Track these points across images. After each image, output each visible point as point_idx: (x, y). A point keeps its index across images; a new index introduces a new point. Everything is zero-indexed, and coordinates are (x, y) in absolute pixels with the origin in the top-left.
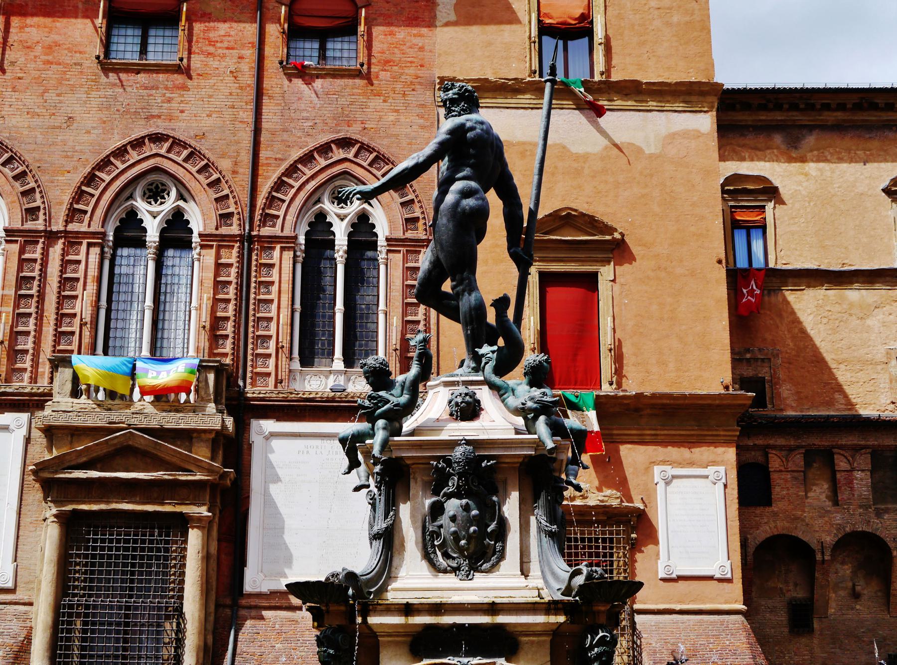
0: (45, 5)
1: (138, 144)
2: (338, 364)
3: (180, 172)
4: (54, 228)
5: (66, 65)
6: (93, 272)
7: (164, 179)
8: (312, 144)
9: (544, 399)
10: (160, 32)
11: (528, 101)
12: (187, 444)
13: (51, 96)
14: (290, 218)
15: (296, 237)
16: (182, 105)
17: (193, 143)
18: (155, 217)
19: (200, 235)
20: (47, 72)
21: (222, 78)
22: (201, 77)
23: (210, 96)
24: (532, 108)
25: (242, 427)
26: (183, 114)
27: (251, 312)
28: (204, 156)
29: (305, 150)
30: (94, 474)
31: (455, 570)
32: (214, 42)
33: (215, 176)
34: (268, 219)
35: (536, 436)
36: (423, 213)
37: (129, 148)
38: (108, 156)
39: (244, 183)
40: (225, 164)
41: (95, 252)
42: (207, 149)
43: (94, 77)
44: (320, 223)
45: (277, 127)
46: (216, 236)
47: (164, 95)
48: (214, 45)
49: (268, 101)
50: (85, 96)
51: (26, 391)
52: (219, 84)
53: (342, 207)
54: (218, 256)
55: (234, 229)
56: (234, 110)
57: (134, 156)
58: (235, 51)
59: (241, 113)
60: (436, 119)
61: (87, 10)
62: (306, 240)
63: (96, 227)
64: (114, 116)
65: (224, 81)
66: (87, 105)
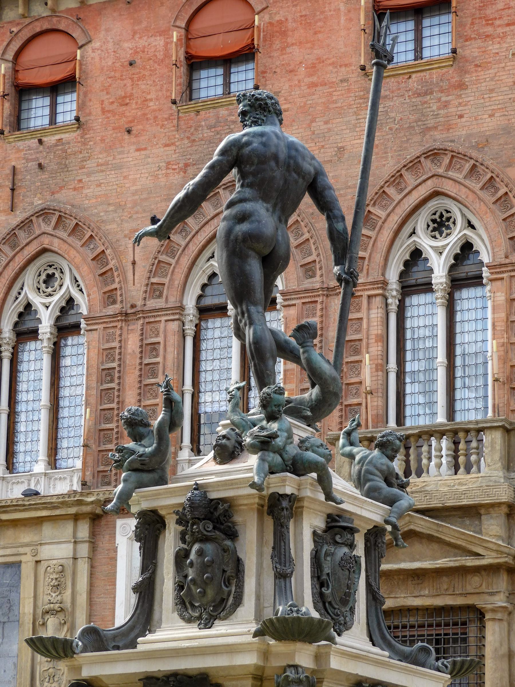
0: (306, 16)
3: (462, 193)
5: (332, 84)
10: (435, 20)
12: (477, 522)
13: (319, 126)
16: (460, 108)
17: (474, 154)
20: (314, 97)
21: (503, 65)
22: (480, 69)
23: (492, 91)
26: (463, 120)
32: (491, 20)
43: (362, 93)
46: (505, 265)
47: (439, 100)
50: (354, 117)
52: (501, 74)
61: (349, 11)
64: (387, 137)
65: (507, 68)
66: (357, 129)
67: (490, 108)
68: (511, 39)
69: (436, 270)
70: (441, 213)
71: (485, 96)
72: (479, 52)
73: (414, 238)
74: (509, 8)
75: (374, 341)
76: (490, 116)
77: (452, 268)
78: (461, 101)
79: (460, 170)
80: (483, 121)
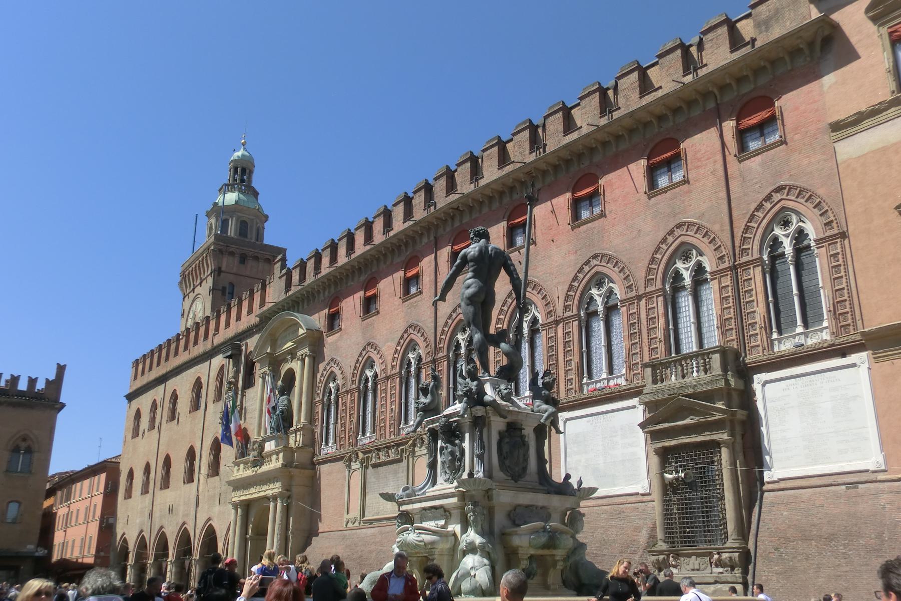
1: (671, 232)
2: (800, 329)
4: (640, 293)
6: (661, 311)
8: (761, 197)
14: (756, 247)
25: (749, 382)
27: (743, 311)
29: (758, 203)
30: (666, 425)
34: (744, 251)
36: (835, 216)
40: (716, 228)
44: (776, 243)
51: (640, 385)
53: (787, 230)
54: (720, 283)
55: (726, 265)
76: (704, 203)
77: (694, 277)
79: (692, 230)
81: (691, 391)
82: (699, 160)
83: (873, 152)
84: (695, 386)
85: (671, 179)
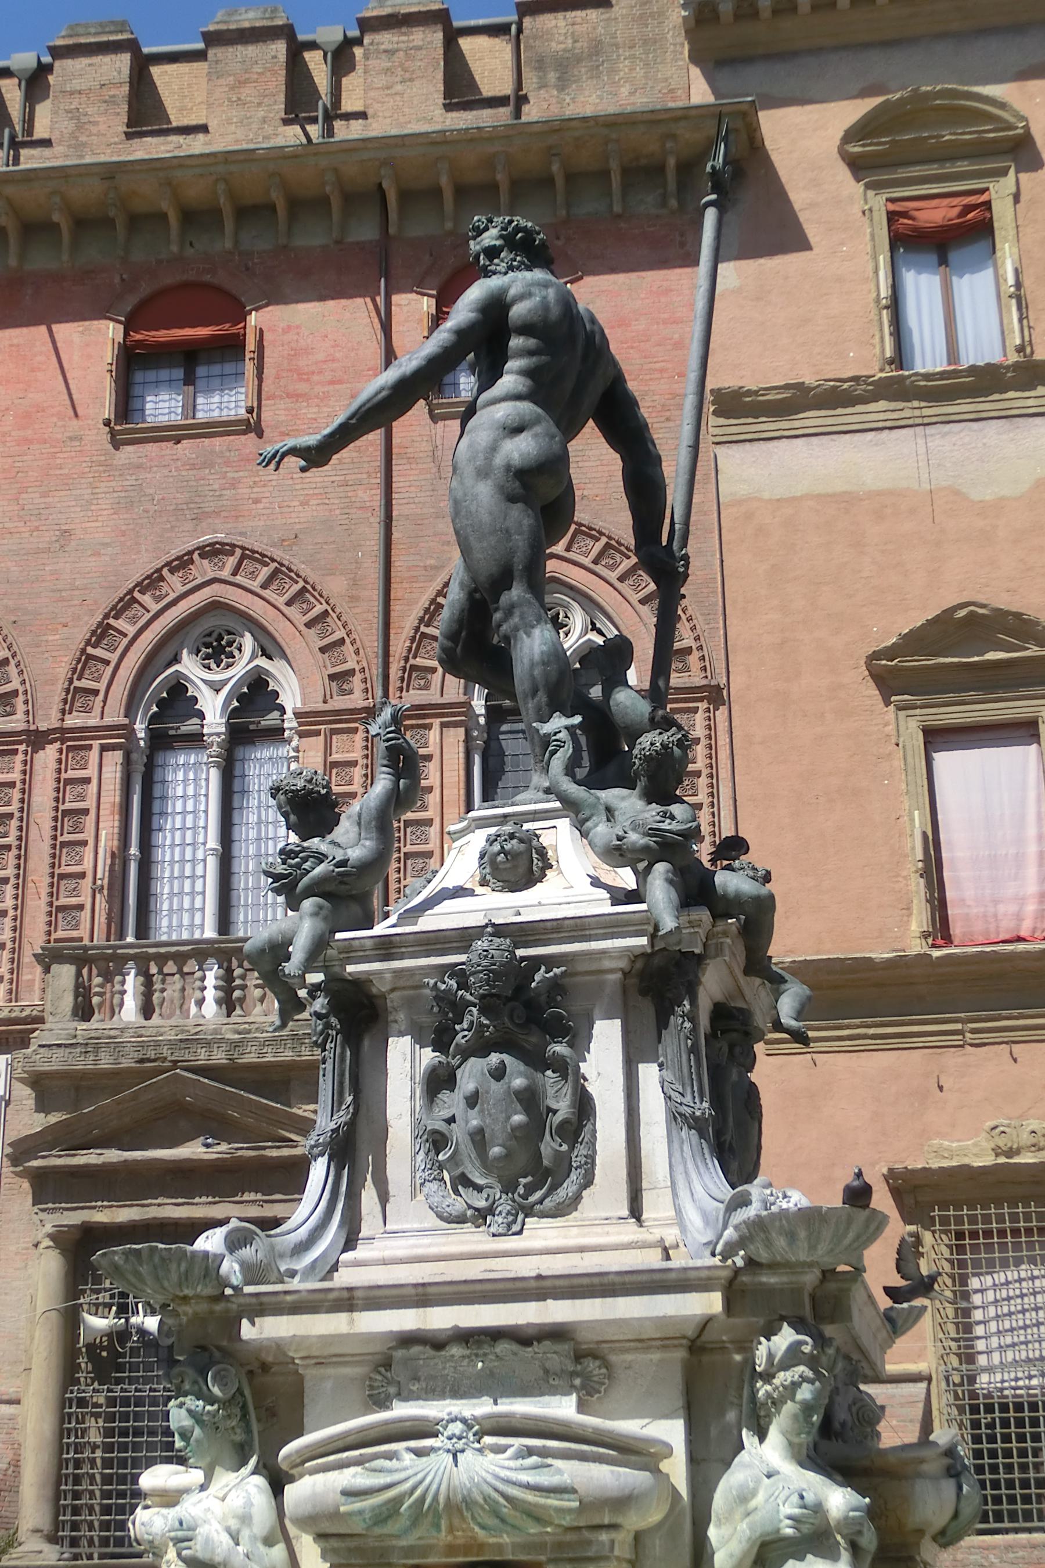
0: (18, 345)
1: (182, 563)
4: (43, 726)
6: (112, 794)
7: (230, 623)
9: (665, 826)
11: (882, 416)
15: (468, 705)
16: (255, 490)
17: (277, 554)
18: (218, 691)
19: (297, 715)
24: (891, 428)
28: (298, 576)
30: (113, 1155)
31: (481, 1216)
32: (307, 374)
33: (318, 609)
35: (643, 907)
36: (697, 639)
37: (165, 572)
38: (131, 592)
39: (370, 616)
40: (334, 586)
41: (115, 758)
42: (303, 563)
43: (103, 458)
45: (425, 511)
48: (308, 380)
49: (407, 467)
50: (89, 491)
54: (328, 749)
55: (357, 700)
56: (348, 489)
57: (175, 584)
58: (344, 386)
59: (360, 493)
60: (713, 466)
62: (487, 707)
63: (115, 716)
64: (140, 521)
66: (93, 507)
67: (302, 492)
68: (336, 401)
69: (209, 718)
70: (220, 634)
71: (295, 476)
72: (286, 415)
73: (176, 667)
74: (333, 360)
75: (108, 812)
77: (234, 714)
78: (257, 479)
79: (253, 576)
80: (291, 509)
81: (219, 1057)
82: (304, 376)
83: (819, 497)
84: (235, 1045)
85: (190, 408)
